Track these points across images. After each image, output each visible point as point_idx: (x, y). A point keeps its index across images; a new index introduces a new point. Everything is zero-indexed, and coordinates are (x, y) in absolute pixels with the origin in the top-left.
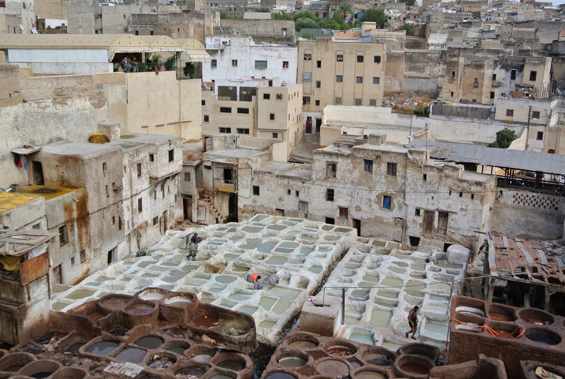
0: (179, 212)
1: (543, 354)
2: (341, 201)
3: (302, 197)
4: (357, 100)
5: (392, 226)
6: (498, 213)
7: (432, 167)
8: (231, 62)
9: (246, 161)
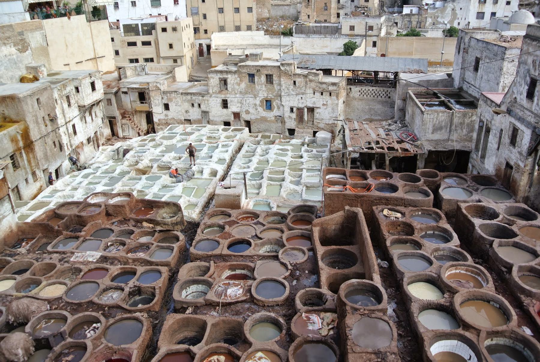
0: (107, 131)
1: (387, 200)
2: (234, 108)
4: (236, 27)
5: (274, 122)
6: (349, 105)
7: (299, 75)
8: (131, 4)
9: (155, 84)
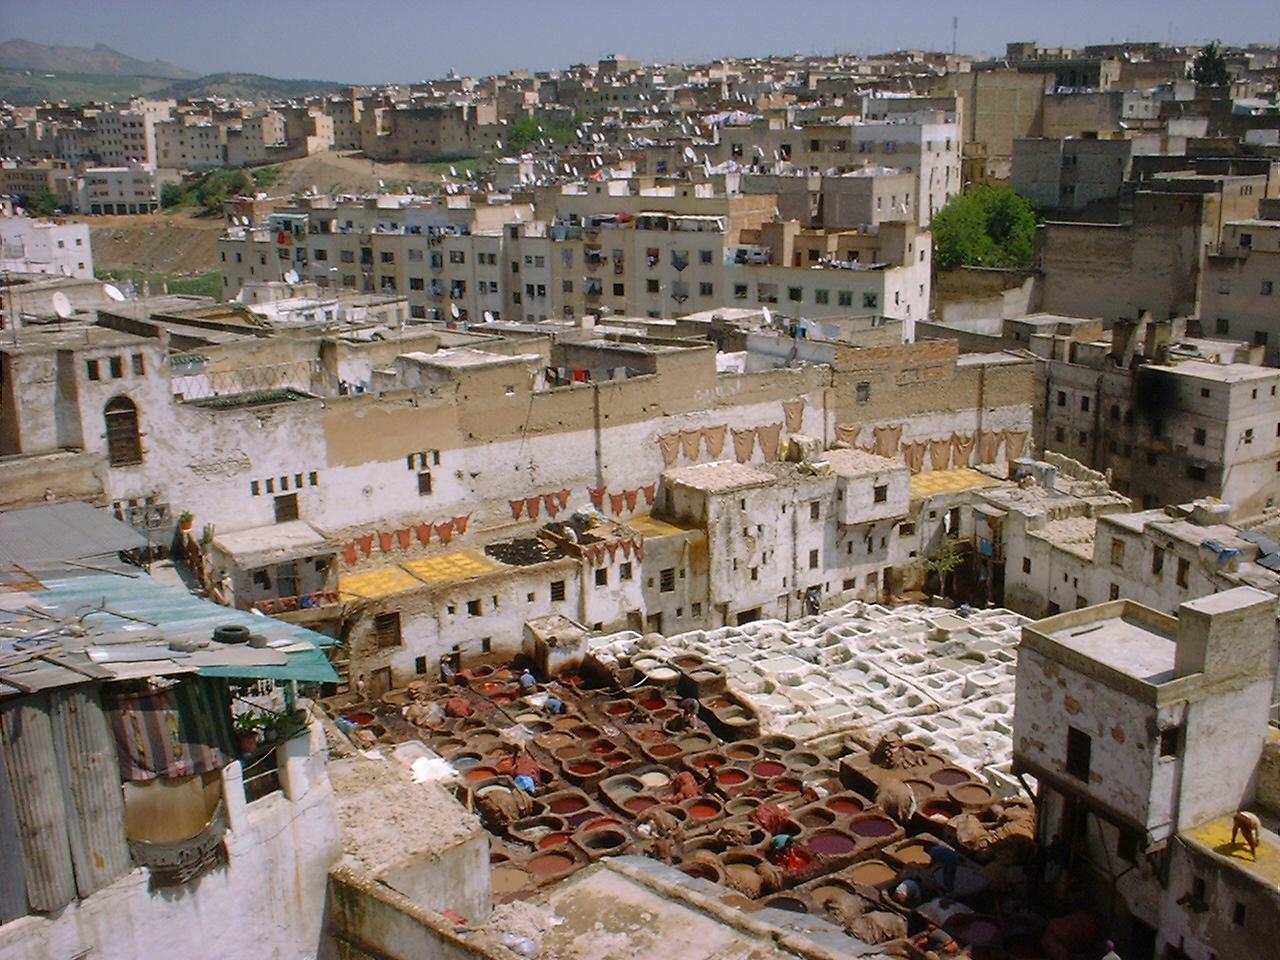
3: (1081, 590)
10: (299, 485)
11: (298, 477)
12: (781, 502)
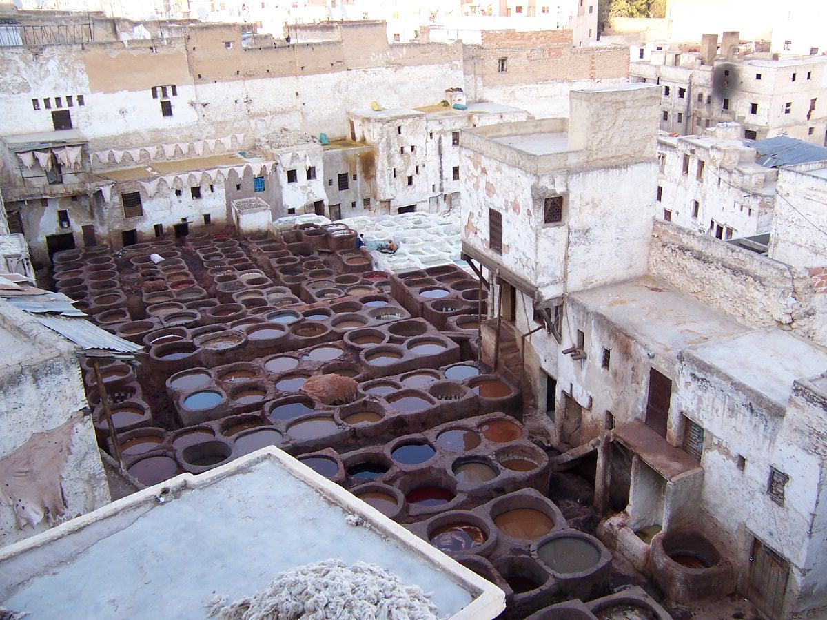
10: (70, 104)
11: (69, 98)
12: (429, 131)
